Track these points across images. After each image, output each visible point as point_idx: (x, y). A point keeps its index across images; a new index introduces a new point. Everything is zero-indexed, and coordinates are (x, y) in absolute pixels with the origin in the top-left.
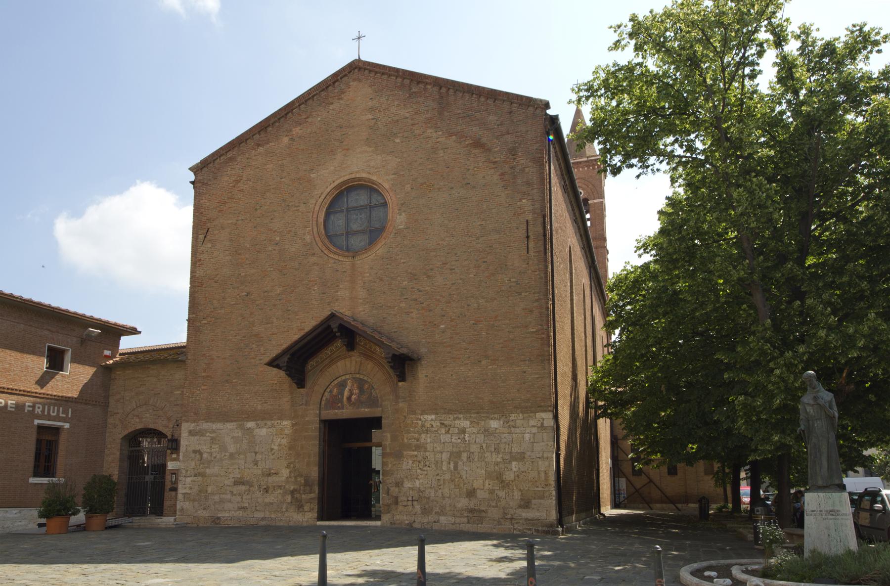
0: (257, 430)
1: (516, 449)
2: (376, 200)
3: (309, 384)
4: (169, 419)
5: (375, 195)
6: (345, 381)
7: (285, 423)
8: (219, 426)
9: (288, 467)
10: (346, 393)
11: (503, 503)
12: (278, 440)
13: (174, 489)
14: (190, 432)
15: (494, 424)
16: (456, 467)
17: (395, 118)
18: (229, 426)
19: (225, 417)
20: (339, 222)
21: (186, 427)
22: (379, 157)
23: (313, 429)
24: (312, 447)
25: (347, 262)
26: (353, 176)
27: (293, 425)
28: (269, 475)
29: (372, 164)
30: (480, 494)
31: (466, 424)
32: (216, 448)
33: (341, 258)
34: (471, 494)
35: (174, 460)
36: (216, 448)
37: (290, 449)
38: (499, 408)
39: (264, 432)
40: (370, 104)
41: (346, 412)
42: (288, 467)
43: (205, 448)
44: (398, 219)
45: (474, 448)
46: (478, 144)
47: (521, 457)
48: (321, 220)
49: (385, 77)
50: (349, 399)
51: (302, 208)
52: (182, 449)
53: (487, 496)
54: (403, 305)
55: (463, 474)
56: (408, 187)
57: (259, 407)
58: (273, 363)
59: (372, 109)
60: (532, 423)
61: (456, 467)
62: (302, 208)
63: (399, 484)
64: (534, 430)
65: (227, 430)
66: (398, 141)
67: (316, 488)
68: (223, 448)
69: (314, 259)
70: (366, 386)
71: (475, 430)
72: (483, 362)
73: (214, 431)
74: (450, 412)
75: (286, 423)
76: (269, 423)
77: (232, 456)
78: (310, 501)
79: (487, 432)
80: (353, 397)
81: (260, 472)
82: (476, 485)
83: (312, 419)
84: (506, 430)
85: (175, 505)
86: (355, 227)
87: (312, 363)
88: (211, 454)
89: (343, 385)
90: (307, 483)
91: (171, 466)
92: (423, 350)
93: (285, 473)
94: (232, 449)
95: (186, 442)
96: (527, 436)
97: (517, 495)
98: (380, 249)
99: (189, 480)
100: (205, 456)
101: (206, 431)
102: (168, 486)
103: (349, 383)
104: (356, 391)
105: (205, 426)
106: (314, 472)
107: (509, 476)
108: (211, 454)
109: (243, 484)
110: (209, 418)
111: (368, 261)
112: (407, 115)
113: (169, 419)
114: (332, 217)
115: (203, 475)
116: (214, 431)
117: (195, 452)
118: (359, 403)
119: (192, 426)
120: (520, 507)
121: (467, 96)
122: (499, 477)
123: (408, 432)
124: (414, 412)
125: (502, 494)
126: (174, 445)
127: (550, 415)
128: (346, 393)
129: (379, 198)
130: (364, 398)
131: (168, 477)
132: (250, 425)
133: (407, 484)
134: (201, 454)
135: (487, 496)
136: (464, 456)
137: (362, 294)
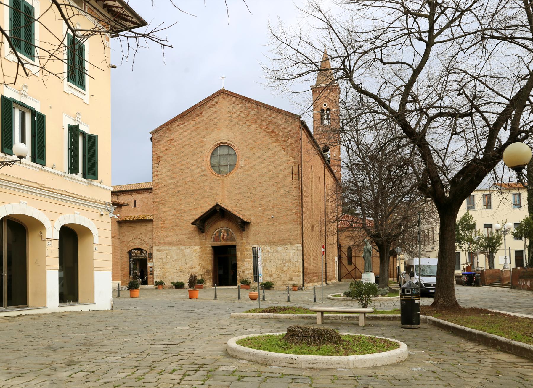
0: (186, 250)
1: (288, 258)
2: (231, 152)
3: (206, 231)
4: (147, 245)
5: (231, 150)
6: (221, 230)
7: (197, 247)
8: (170, 248)
9: (199, 265)
10: (222, 235)
11: (283, 279)
12: (194, 254)
13: (152, 274)
14: (157, 250)
15: (279, 249)
16: (265, 265)
17: (239, 117)
18: (174, 248)
19: (172, 244)
20: (215, 160)
21: (155, 248)
22: (233, 134)
23: (209, 250)
24: (209, 257)
25: (221, 179)
26: (222, 141)
27: (201, 248)
28: (192, 268)
29: (230, 137)
30: (274, 276)
31: (269, 248)
32: (169, 257)
33: (218, 178)
34: (271, 275)
35: (151, 262)
36: (169, 257)
37: (200, 258)
38: (281, 242)
39: (188, 251)
40: (228, 109)
41: (222, 243)
42: (199, 265)
43: (164, 257)
44: (242, 162)
45: (272, 258)
46: (273, 132)
47: (289, 261)
48: (209, 160)
49: (234, 98)
50: (223, 238)
51: (200, 154)
52: (154, 257)
53: (277, 276)
54: (244, 199)
55: (268, 268)
56: (245, 148)
57: (186, 240)
58: (192, 224)
59: (230, 112)
60: (294, 248)
61: (265, 265)
62: (200, 154)
63: (244, 272)
64: (294, 251)
65: (173, 250)
66: (240, 127)
67: (211, 274)
68: (172, 257)
69: (205, 178)
70: (229, 233)
71: (272, 251)
72: (276, 224)
73: (167, 250)
74: (263, 243)
75: (198, 247)
76: (191, 247)
77: (175, 260)
78: (209, 279)
79: (277, 251)
80: (225, 237)
81: (187, 267)
82: (273, 272)
83: (209, 244)
84: (284, 251)
85: (153, 280)
86: (223, 163)
87: (207, 222)
88: (167, 259)
89: (220, 232)
90: (208, 271)
91: (149, 264)
92: (252, 218)
93: (198, 267)
94: (175, 257)
95: (155, 255)
96: (292, 253)
97: (288, 276)
98: (233, 175)
99: (158, 270)
100: (164, 260)
101: (164, 250)
102: (149, 272)
103: (223, 231)
104: (226, 235)
105: (163, 248)
106: (210, 267)
107: (285, 268)
108: (167, 259)
109: (181, 272)
110: (165, 244)
111: (228, 179)
112: (244, 116)
113: (147, 245)
114: (213, 158)
115: (164, 268)
116: (167, 250)
117: (160, 259)
118: (227, 240)
119: (158, 248)
120: (289, 280)
121: (268, 110)
122: (281, 269)
123: (247, 251)
124: (249, 244)
125: (282, 275)
126: (151, 256)
127: (301, 245)
128: (222, 235)
129: (233, 151)
130: (229, 237)
131: (149, 269)
132: (183, 248)
133: (247, 272)
134: (162, 260)
135: (277, 276)
136: (268, 261)
137: (227, 194)
